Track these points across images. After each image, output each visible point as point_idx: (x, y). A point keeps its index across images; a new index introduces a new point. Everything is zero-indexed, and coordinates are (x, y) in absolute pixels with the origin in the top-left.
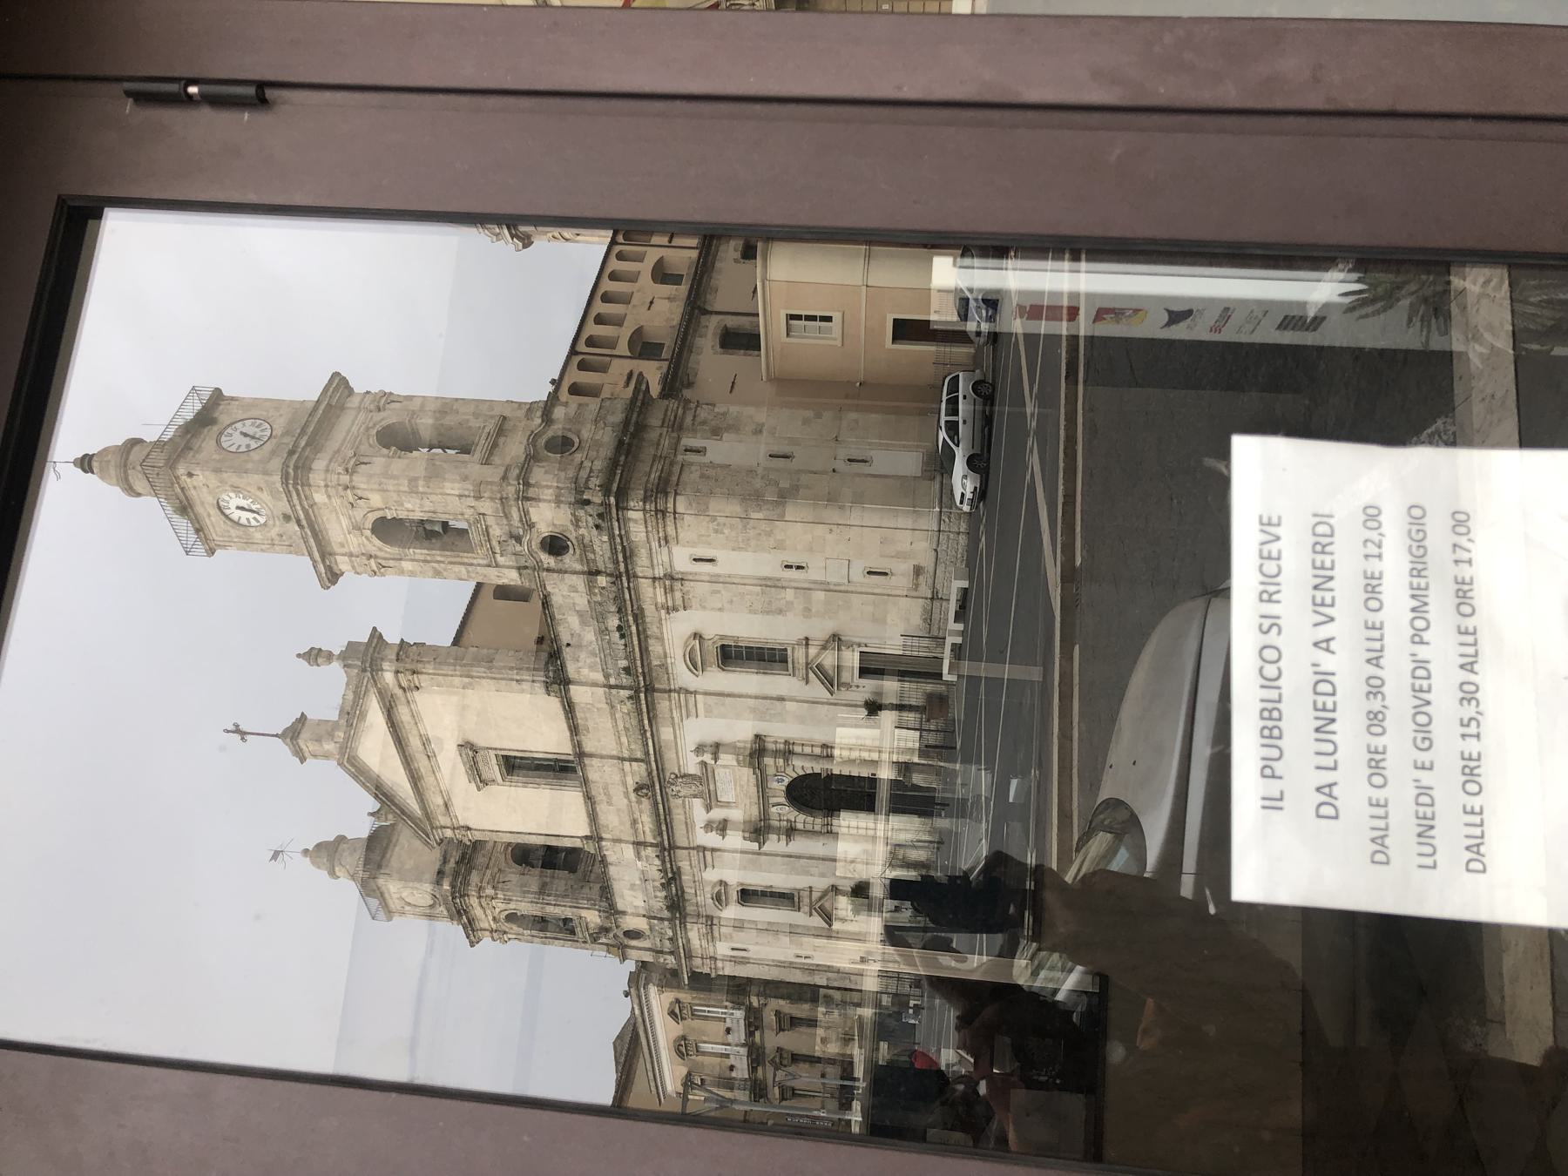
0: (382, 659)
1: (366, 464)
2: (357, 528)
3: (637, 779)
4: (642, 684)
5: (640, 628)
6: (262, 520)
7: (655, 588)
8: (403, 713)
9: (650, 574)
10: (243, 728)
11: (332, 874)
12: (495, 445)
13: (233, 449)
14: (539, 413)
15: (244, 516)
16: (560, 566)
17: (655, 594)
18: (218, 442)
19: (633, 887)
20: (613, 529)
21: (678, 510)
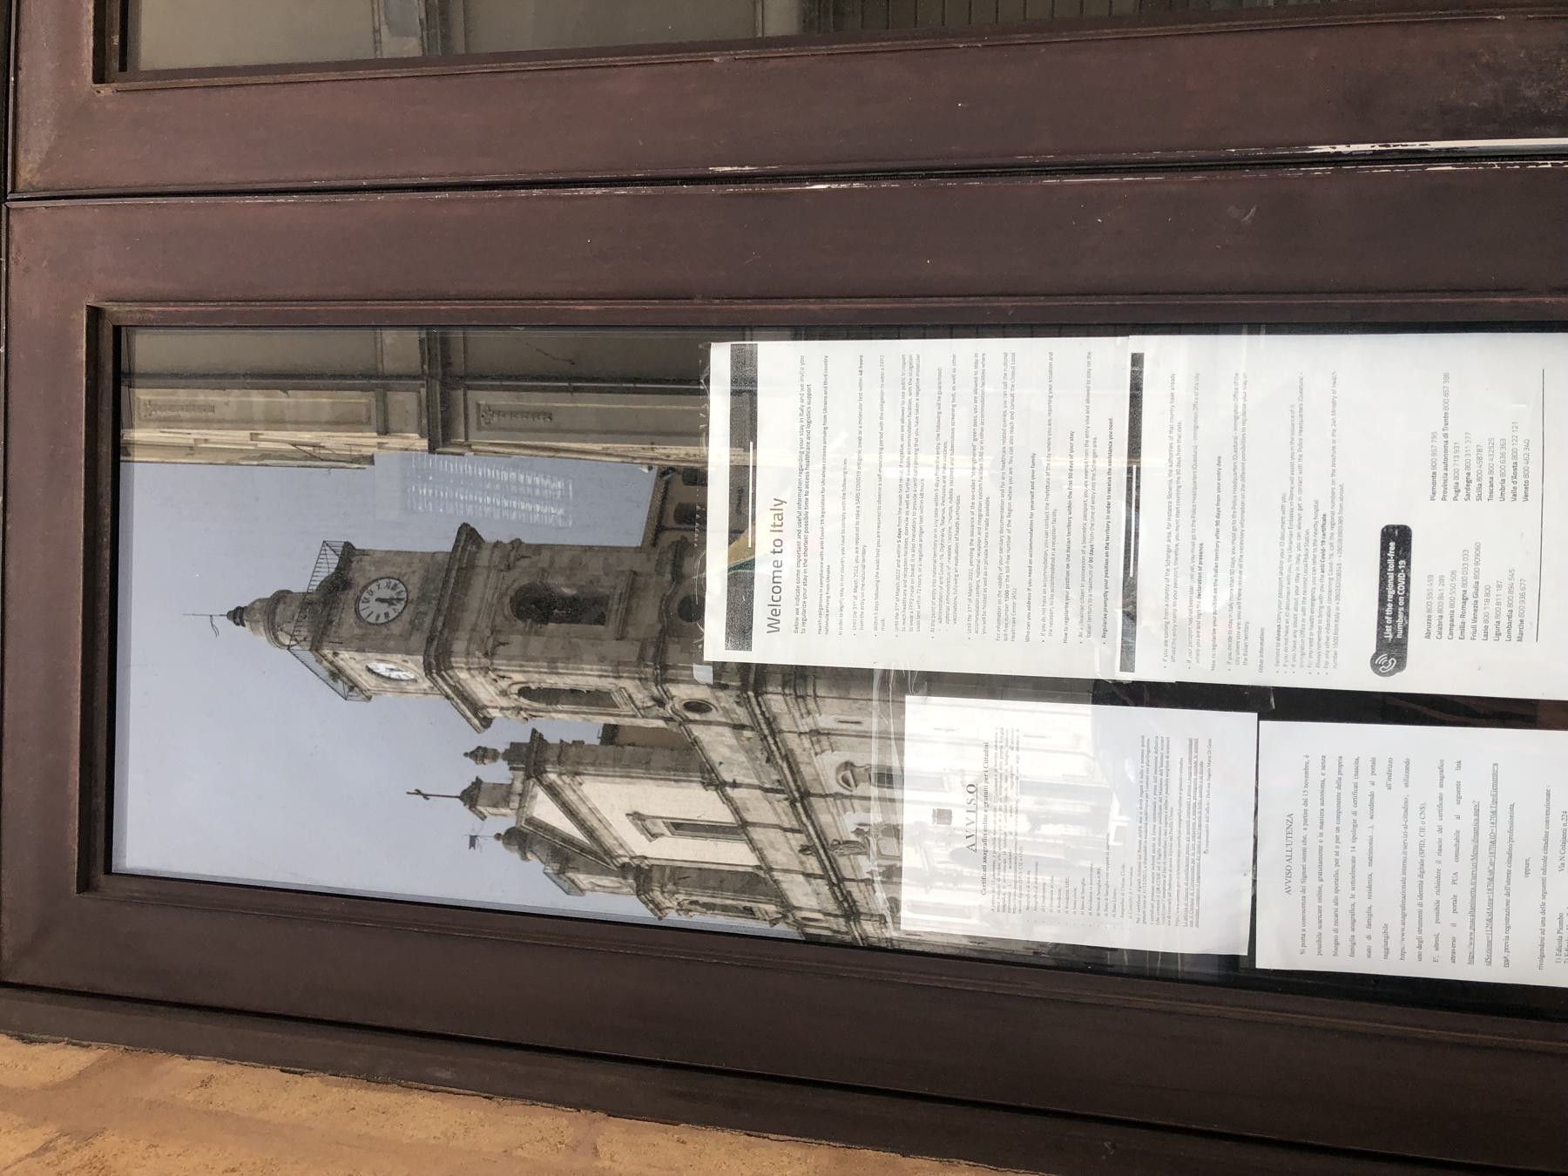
0: (546, 761)
1: (503, 644)
2: (504, 693)
3: (802, 843)
4: (797, 795)
5: (790, 760)
6: (412, 677)
7: (801, 740)
8: (570, 796)
9: (796, 730)
10: (423, 791)
11: (524, 858)
12: (628, 611)
13: (372, 619)
14: (668, 568)
15: (394, 675)
16: (704, 719)
17: (802, 744)
18: (357, 612)
19: (806, 895)
20: (753, 710)
21: (819, 694)
